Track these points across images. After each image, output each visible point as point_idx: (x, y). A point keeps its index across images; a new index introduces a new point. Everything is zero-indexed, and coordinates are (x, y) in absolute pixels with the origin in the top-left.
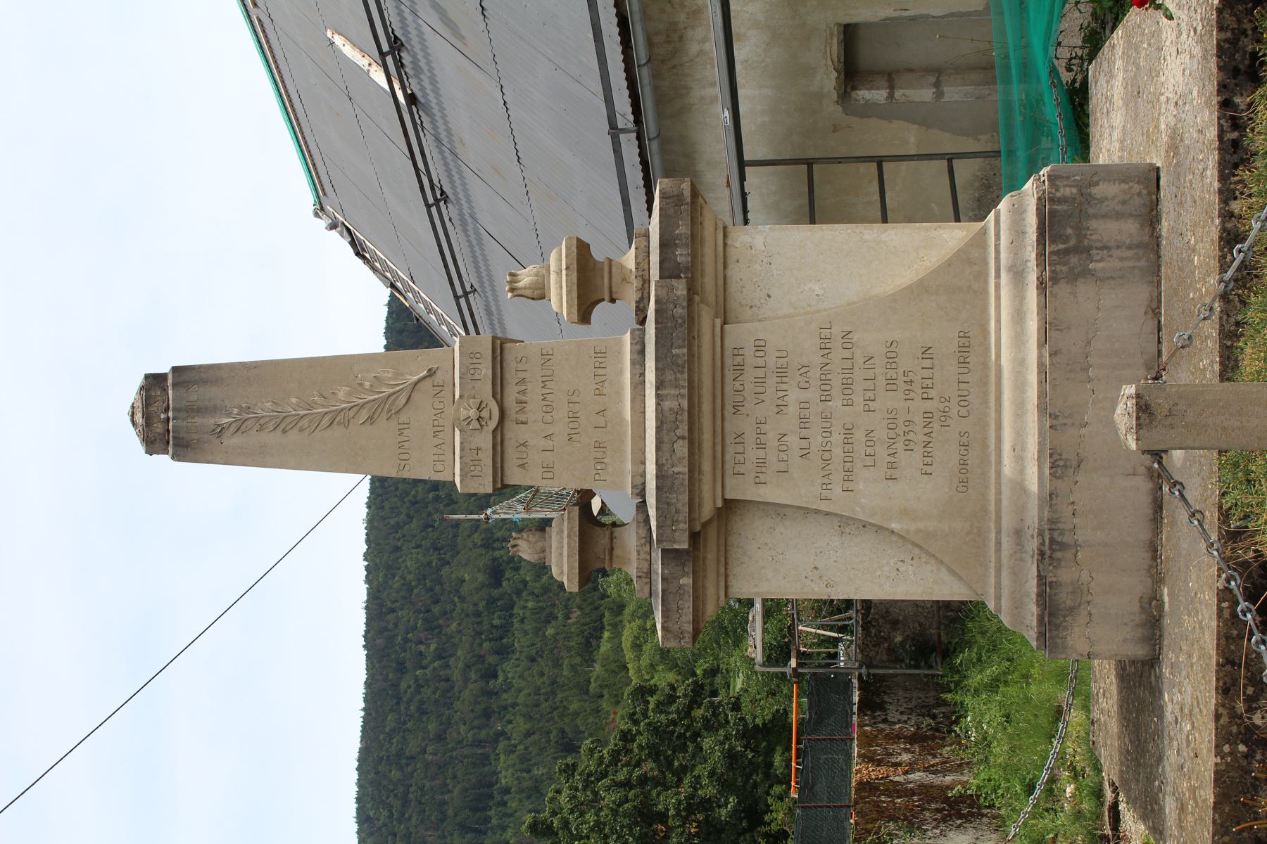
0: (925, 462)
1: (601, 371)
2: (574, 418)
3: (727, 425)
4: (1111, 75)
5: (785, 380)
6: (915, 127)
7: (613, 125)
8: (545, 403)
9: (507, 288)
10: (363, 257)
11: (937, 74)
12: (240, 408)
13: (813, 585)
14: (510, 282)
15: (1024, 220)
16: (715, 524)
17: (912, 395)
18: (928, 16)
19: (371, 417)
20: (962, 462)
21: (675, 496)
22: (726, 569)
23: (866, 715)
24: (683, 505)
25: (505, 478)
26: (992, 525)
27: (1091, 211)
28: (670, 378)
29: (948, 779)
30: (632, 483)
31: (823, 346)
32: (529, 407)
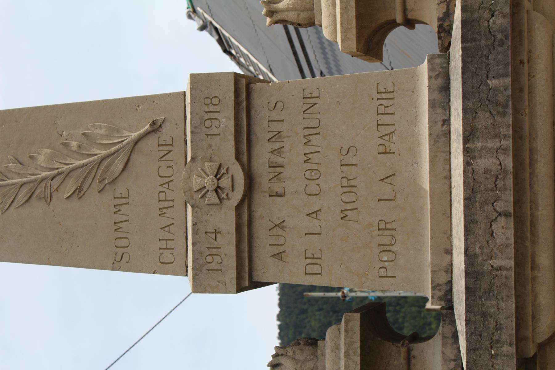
1: (387, 119)
8: (309, 166)
9: (264, 11)
10: (230, 54)
19: (79, 189)
21: (494, 302)
24: (507, 318)
25: (254, 273)
28: (484, 123)
30: (432, 282)
32: (287, 172)
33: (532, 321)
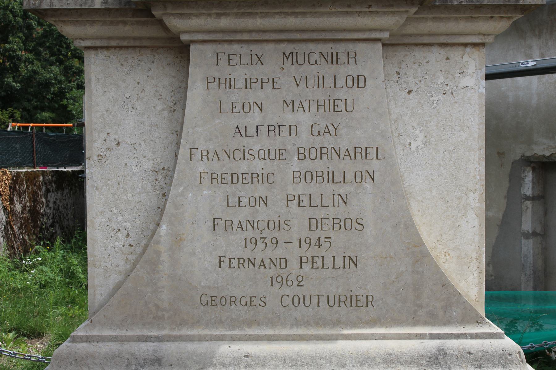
0: (232, 261)
3: (271, 46)
5: (321, 110)
6: (501, 218)
13: (101, 141)
15: (494, 366)
16: (162, 34)
17: (305, 246)
20: (233, 299)
22: (115, 47)
23: (52, 176)
26: (165, 332)
31: (358, 150)
33: (178, 14)
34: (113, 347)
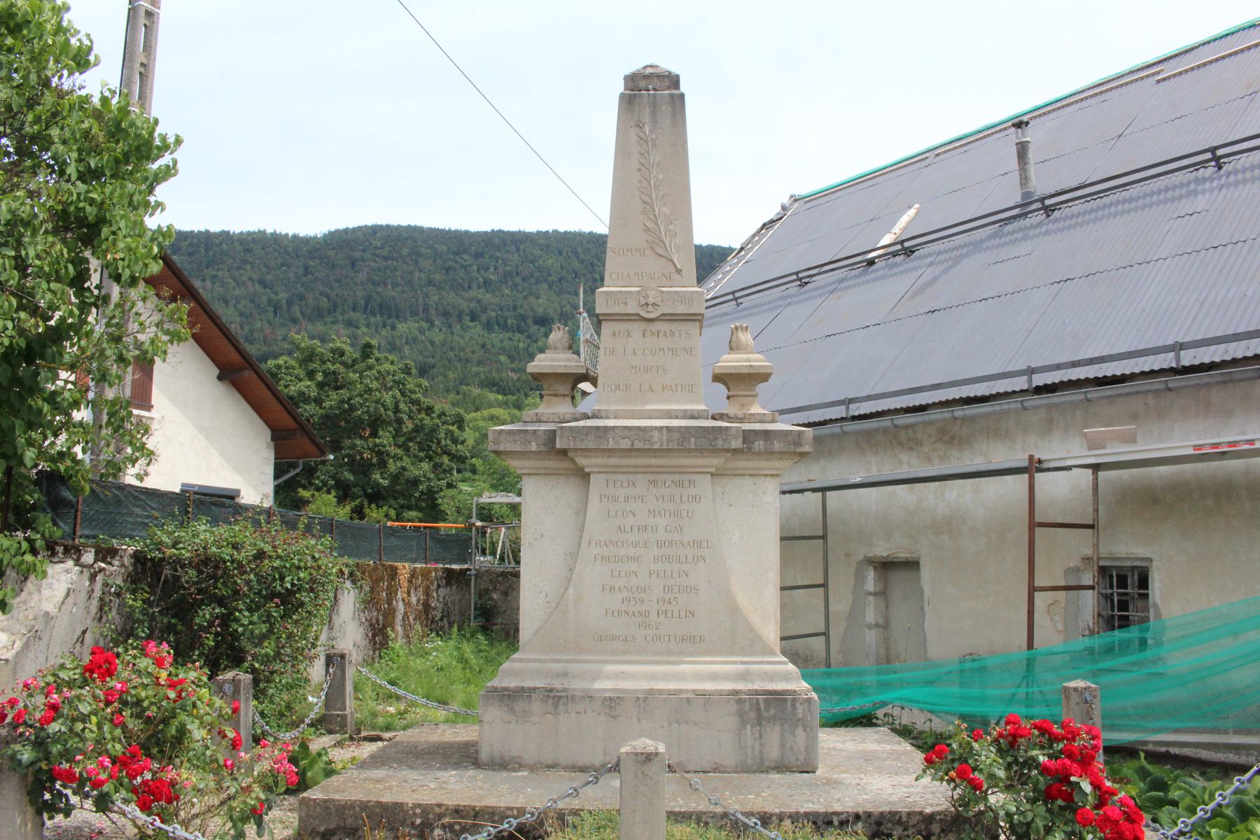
1: (679, 389)
2: (647, 370)
3: (640, 476)
4: (880, 742)
6: (848, 609)
7: (851, 401)
10: (762, 228)
11: (884, 626)
12: (656, 140)
14: (742, 327)
16: (572, 466)
18: (924, 619)
26: (571, 657)
27: (786, 727)
29: (399, 628)
34: (538, 665)
